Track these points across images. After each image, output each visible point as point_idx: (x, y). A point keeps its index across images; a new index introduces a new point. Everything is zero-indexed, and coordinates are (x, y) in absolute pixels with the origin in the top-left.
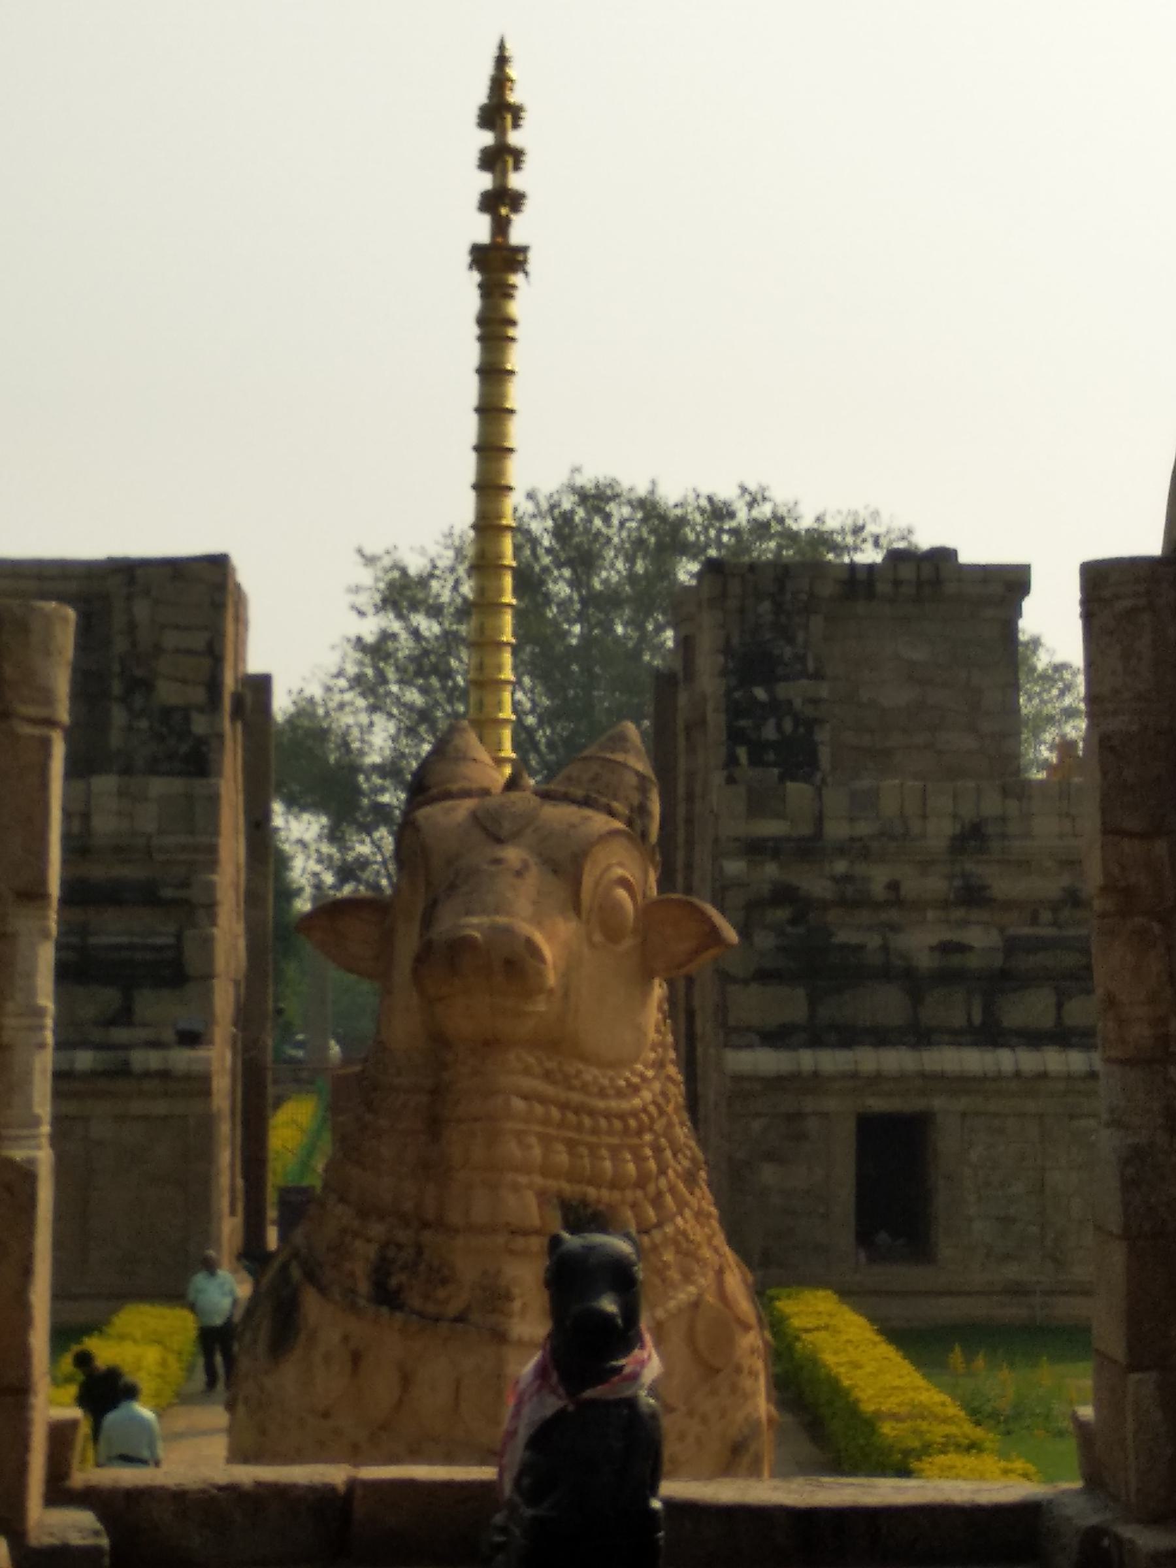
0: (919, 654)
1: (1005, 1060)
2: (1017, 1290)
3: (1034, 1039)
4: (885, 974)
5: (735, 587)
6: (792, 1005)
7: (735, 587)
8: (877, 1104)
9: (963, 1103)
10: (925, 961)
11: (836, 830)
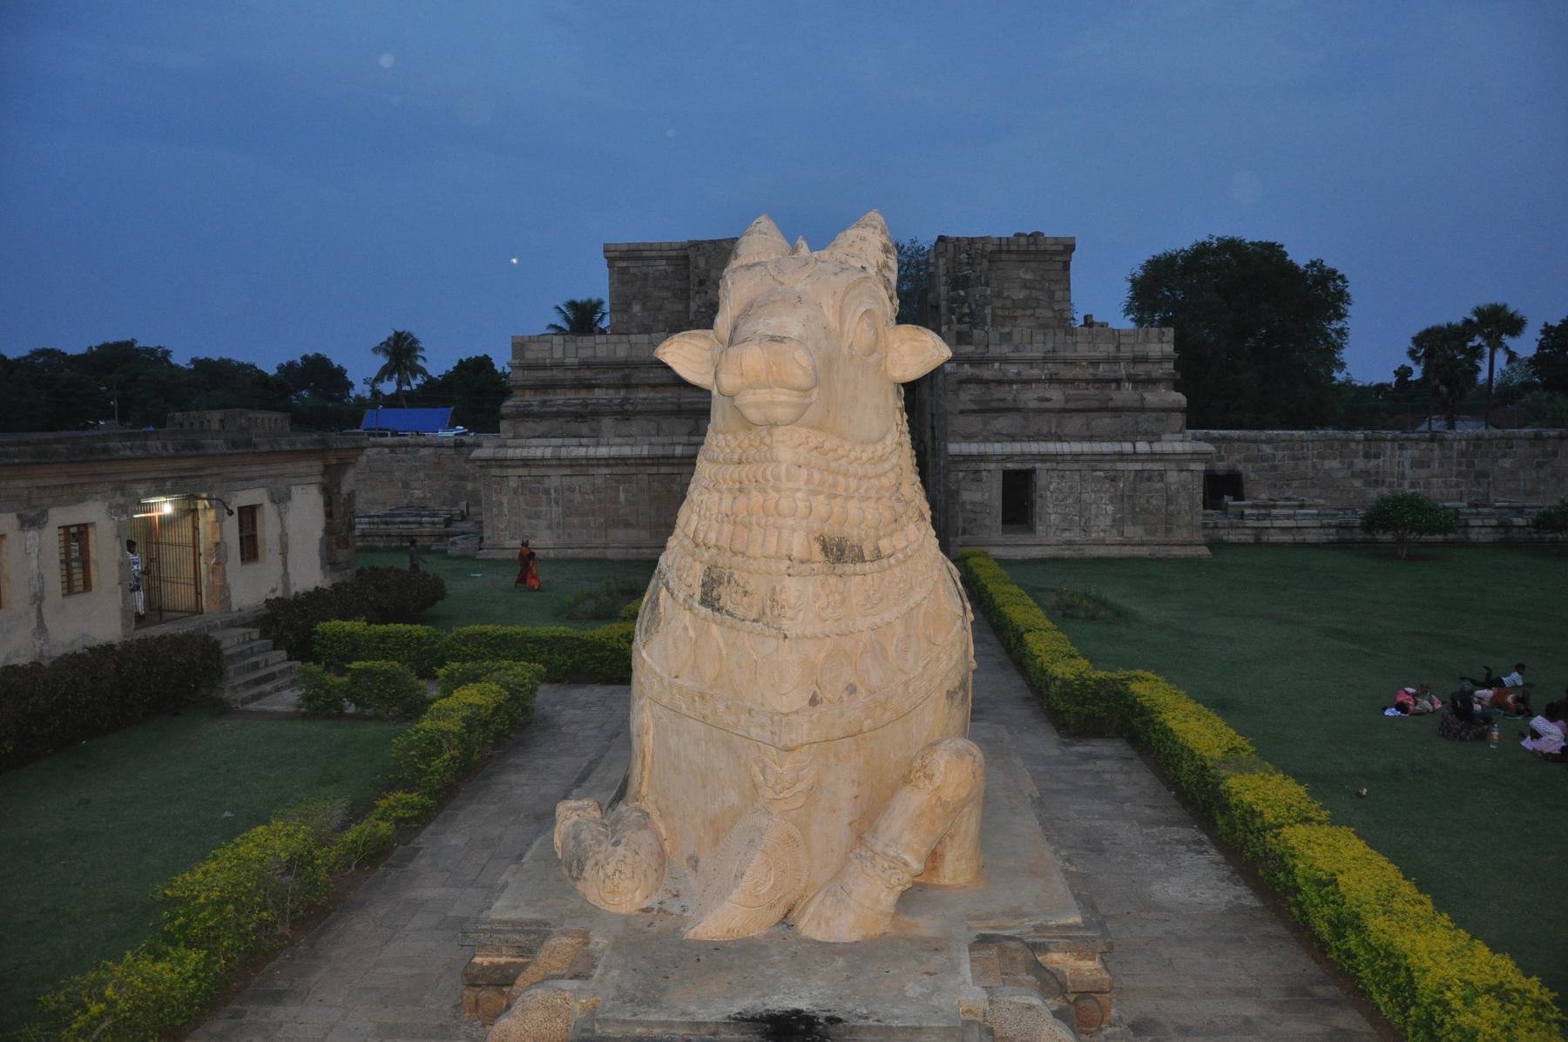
0: (1029, 276)
1: (1065, 447)
2: (1070, 543)
4: (1018, 410)
5: (951, 247)
6: (975, 423)
7: (951, 247)
8: (1010, 466)
9: (1048, 465)
10: (1033, 404)
11: (994, 351)
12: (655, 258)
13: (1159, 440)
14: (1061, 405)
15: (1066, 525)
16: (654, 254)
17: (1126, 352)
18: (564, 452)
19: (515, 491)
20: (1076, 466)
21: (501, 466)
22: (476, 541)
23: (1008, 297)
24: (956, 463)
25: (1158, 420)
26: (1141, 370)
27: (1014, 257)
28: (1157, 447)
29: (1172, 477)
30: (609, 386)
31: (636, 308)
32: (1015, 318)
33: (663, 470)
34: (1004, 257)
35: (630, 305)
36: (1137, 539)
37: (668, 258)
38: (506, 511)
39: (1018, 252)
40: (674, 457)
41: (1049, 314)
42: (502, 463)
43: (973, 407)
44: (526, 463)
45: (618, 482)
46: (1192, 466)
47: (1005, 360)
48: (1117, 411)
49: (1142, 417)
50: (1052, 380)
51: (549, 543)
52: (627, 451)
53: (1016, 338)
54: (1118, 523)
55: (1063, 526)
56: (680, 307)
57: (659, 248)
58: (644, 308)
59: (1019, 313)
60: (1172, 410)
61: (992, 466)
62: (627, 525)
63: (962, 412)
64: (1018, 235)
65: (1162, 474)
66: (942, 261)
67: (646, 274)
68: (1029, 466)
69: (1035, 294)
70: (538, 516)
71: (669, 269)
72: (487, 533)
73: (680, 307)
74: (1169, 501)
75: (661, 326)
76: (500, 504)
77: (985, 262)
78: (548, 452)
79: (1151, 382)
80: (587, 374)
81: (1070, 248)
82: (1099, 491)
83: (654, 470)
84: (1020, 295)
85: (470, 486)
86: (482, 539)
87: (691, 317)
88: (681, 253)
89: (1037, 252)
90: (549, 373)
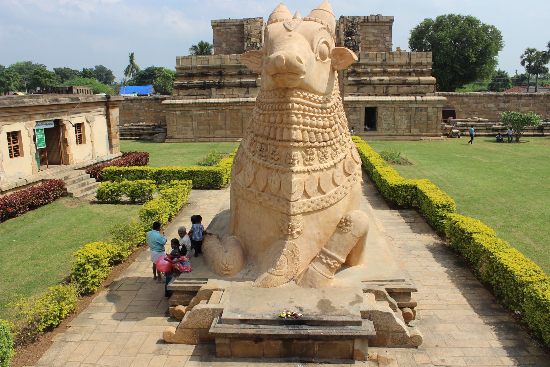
3: (394, 95)
5: (345, 20)
6: (355, 89)
7: (345, 20)
8: (368, 106)
9: (382, 105)
10: (376, 82)
12: (230, 26)
13: (425, 96)
14: (388, 82)
15: (389, 128)
16: (230, 24)
17: (413, 61)
18: (198, 101)
19: (179, 116)
20: (393, 106)
21: (173, 107)
22: (164, 135)
23: (368, 40)
24: (347, 104)
25: (425, 87)
26: (418, 69)
27: (370, 24)
28: (425, 98)
29: (430, 110)
30: (214, 75)
31: (224, 45)
32: (370, 48)
33: (235, 108)
34: (366, 24)
35: (221, 44)
36: (416, 134)
37: (236, 25)
38: (175, 124)
39: (372, 22)
40: (239, 102)
41: (383, 46)
42: (173, 105)
43: (354, 83)
44: (182, 105)
45: (218, 112)
46: (438, 106)
47: (367, 65)
48: (409, 84)
49: (418, 86)
50: (385, 73)
51: (192, 136)
52: (221, 100)
53: (371, 56)
54: (409, 128)
55: (388, 128)
56: (240, 44)
57: (233, 21)
58: (227, 45)
59: (372, 46)
60: (430, 84)
61: (361, 106)
62: (221, 129)
63: (350, 85)
64: (372, 15)
65: (426, 109)
66: (342, 25)
67: (227, 32)
68: (375, 106)
69: (378, 39)
70: (188, 126)
71: (236, 29)
72: (168, 133)
73: (240, 44)
74: (428, 119)
75: (233, 52)
76: (173, 122)
78: (191, 101)
79: (422, 74)
80: (205, 71)
81: (392, 20)
82: (402, 115)
83: (231, 107)
84: (372, 39)
85: (161, 115)
86: (167, 135)
87: (245, 48)
88: (242, 23)
89: (379, 22)
90: (190, 71)
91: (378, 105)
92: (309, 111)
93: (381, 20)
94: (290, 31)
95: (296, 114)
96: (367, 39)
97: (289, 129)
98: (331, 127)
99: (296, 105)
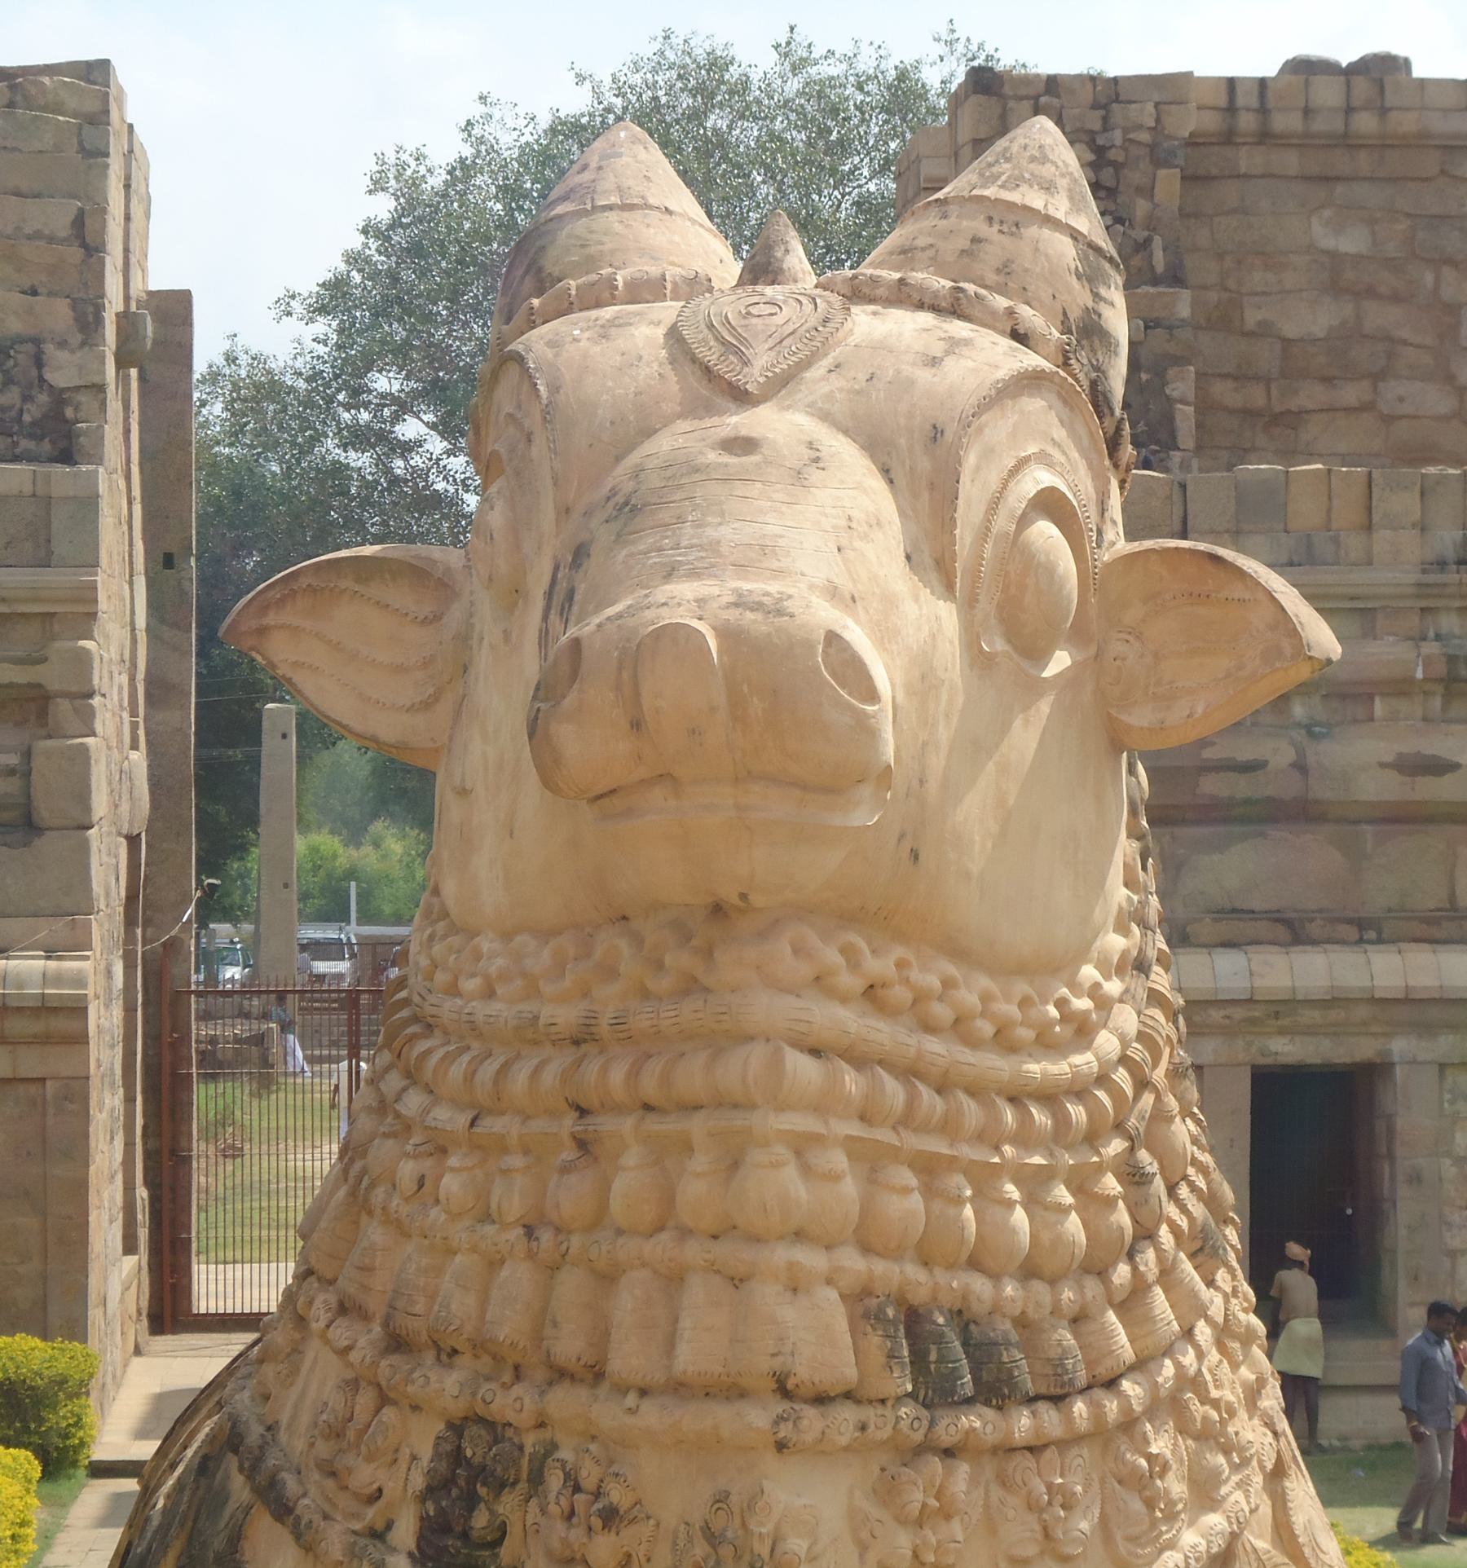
0: (1352, 242)
8: (1286, 1050)
23: (1264, 331)
27: (1290, 162)
32: (1293, 419)
39: (1304, 142)
53: (1306, 511)
59: (1310, 396)
68: (1362, 1049)
69: (1380, 317)
77: (1168, 182)
84: (1313, 319)
91: (1400, 1047)
92: (907, 1120)
93: (1406, 123)
94: (742, 397)
95: (802, 1146)
96: (1253, 317)
97: (737, 1281)
98: (1096, 1268)
99: (803, 1068)
